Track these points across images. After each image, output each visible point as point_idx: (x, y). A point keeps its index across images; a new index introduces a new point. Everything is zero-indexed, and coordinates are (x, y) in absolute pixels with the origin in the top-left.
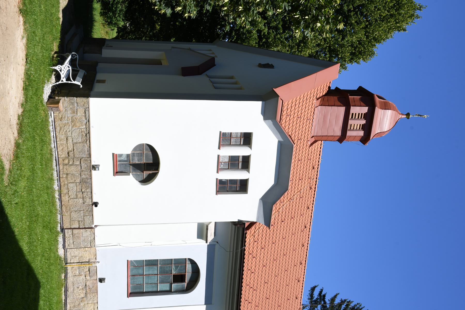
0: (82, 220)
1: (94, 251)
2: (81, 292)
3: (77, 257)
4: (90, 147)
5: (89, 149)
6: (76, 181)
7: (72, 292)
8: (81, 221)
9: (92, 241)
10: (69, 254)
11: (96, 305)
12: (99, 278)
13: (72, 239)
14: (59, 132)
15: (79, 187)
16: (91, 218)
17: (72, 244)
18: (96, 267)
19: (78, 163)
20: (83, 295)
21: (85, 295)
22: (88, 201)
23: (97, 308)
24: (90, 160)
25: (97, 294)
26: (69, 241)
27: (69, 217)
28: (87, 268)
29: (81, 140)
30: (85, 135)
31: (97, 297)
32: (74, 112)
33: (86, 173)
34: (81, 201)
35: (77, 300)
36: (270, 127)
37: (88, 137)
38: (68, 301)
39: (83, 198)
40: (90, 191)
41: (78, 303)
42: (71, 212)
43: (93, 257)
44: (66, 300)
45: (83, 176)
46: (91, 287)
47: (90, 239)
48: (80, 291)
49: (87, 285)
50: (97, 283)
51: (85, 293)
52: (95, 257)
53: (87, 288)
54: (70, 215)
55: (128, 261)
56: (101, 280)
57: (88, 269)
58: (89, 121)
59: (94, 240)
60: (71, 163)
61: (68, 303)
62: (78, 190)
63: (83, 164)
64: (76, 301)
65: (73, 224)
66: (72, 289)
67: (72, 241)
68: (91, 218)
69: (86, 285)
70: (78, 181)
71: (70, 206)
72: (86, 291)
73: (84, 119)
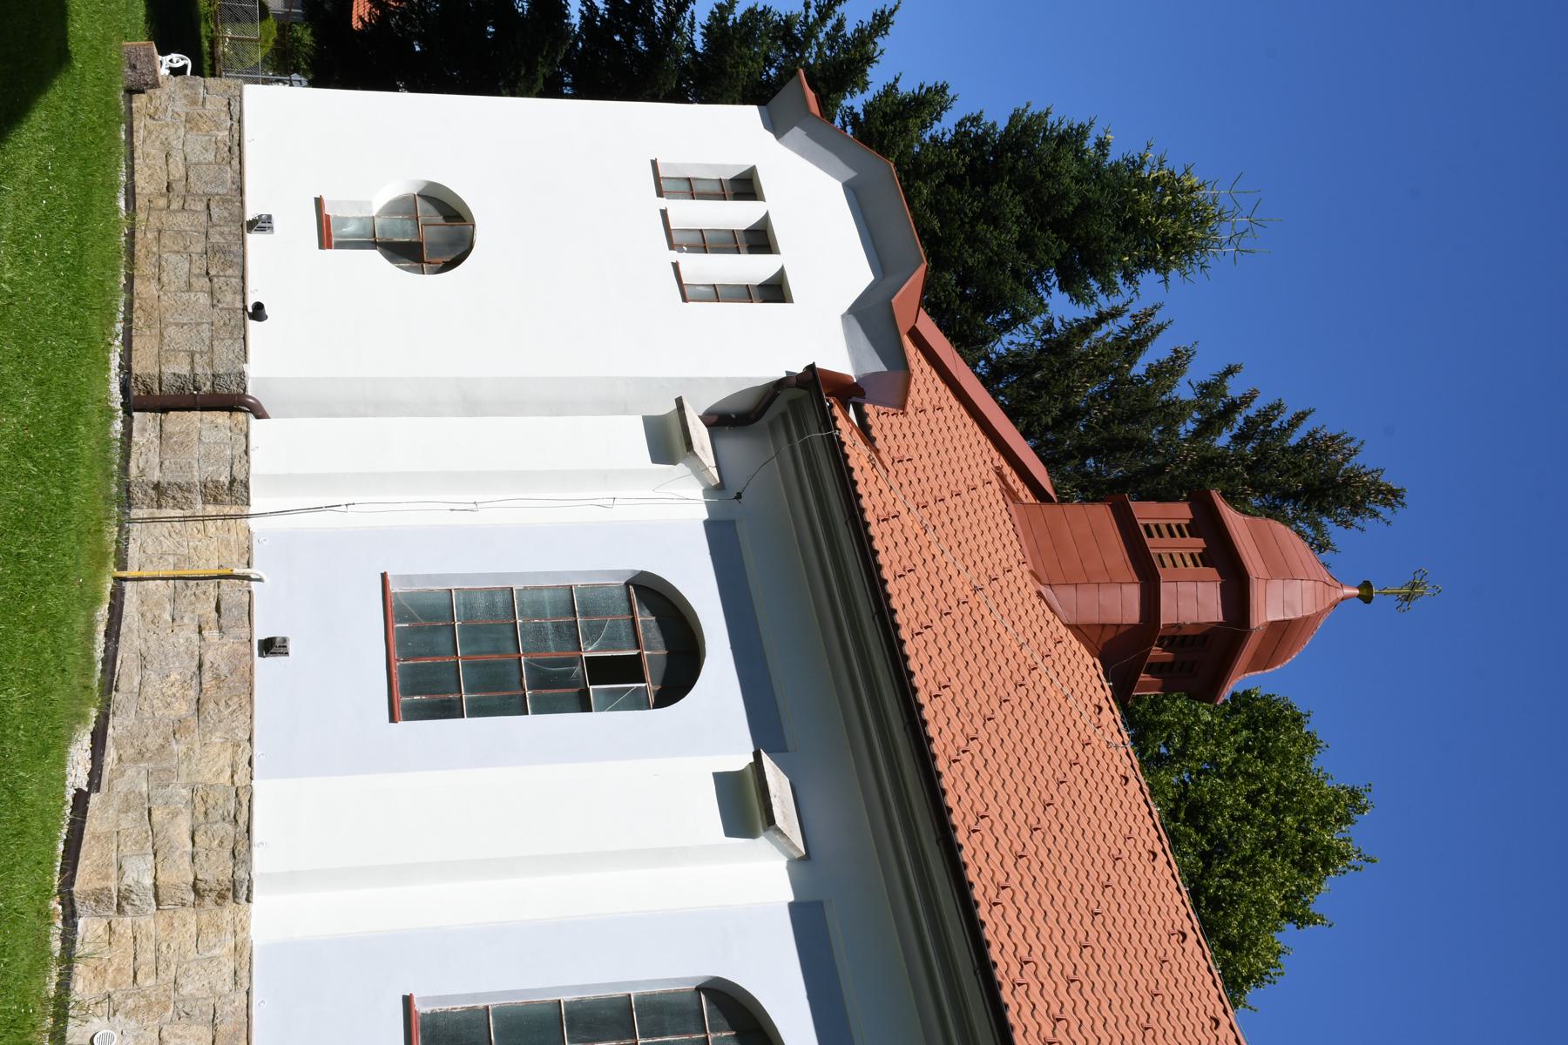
0: (205, 349)
1: (242, 538)
2: (178, 695)
3: (171, 559)
4: (241, 173)
5: (237, 177)
6: (192, 248)
7: (137, 690)
8: (201, 353)
9: (236, 461)
10: (138, 549)
11: (243, 751)
12: (260, 641)
13: (158, 450)
14: (144, 141)
15: (199, 265)
16: (238, 345)
17: (158, 469)
18: (248, 595)
19: (201, 206)
20: (185, 707)
21: (195, 707)
22: (230, 299)
23: (250, 763)
24: (242, 203)
25: (251, 702)
26: (143, 456)
27: (155, 341)
28: (212, 599)
29: (213, 158)
30: (226, 149)
31: (248, 714)
32: (194, 103)
33: (226, 229)
34: (204, 299)
35: (156, 728)
36: (802, 152)
37: (237, 153)
38: (110, 731)
39: (212, 293)
40: (238, 273)
41: (160, 741)
42: (167, 326)
43: (235, 557)
44: (110, 660)
45: (216, 238)
46: (224, 670)
47: (229, 452)
48: (174, 690)
49: (207, 665)
50: (252, 655)
51: (195, 700)
52: (247, 556)
53: (207, 676)
54: (161, 334)
55: (384, 576)
56: (270, 647)
57: (214, 605)
58: (240, 121)
59: (243, 455)
60: (174, 206)
61: (109, 742)
62: (197, 271)
63: (215, 211)
64: (152, 731)
65: (168, 361)
66: (137, 680)
67: (157, 460)
68: (237, 346)
69: (200, 666)
70: (199, 248)
71: (162, 311)
72: (201, 691)
73: (224, 116)
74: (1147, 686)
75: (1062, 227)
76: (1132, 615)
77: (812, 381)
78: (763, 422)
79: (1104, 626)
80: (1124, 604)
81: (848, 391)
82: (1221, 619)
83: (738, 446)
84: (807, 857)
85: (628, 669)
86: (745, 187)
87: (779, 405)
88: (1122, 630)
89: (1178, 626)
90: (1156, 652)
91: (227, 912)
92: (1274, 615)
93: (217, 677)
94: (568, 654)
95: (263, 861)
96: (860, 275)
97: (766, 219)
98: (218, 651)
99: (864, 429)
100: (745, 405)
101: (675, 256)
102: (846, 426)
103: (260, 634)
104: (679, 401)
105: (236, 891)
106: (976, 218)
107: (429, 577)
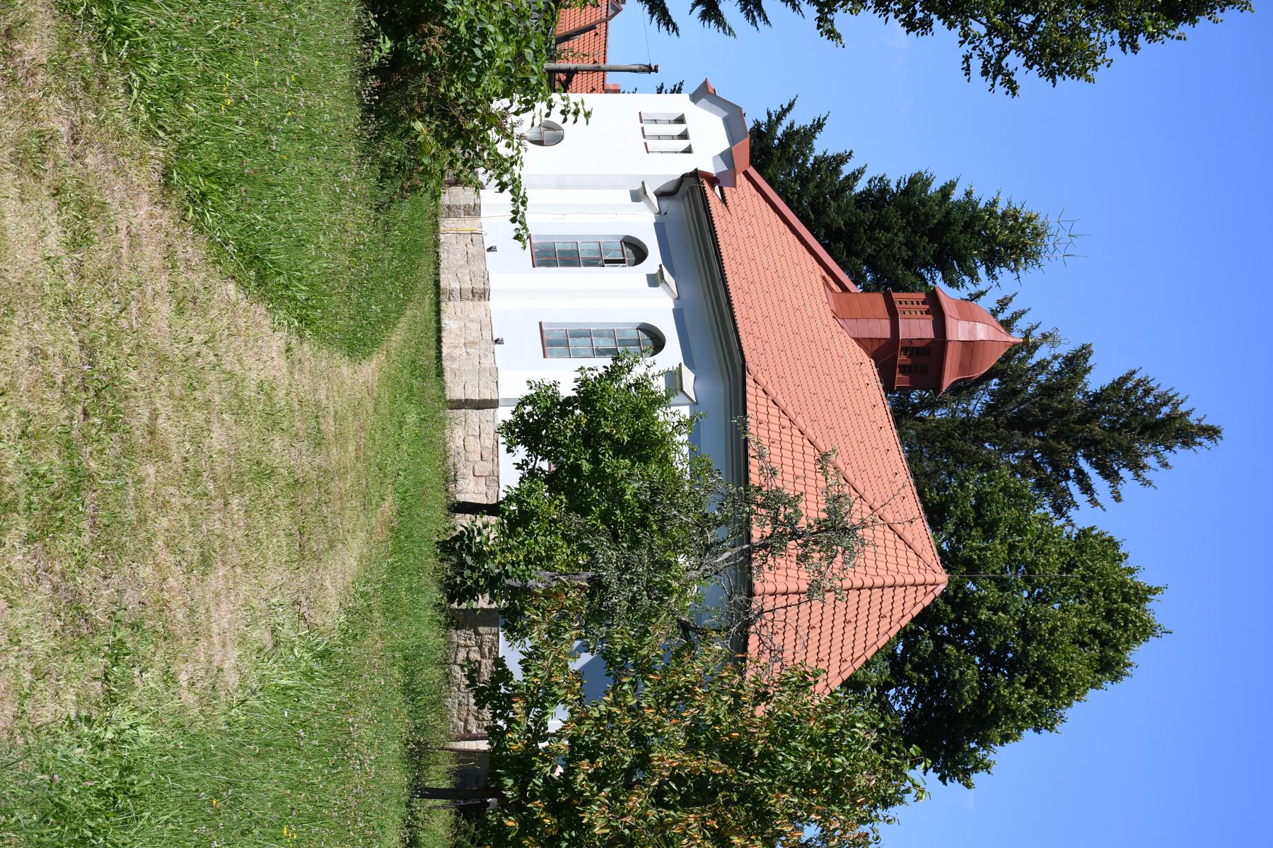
36: (705, 108)
53: (470, 255)
74: (900, 379)
75: (934, 235)
76: (887, 334)
77: (696, 174)
78: (678, 195)
79: (871, 339)
80: (882, 329)
81: (713, 181)
82: (932, 336)
83: (666, 203)
84: (678, 298)
85: (622, 261)
86: (680, 120)
87: (685, 188)
88: (883, 342)
89: (911, 340)
90: (902, 358)
91: (482, 303)
92: (963, 336)
93: (473, 256)
94: (599, 256)
95: (494, 285)
96: (724, 144)
97: (686, 131)
98: (472, 249)
99: (724, 200)
100: (671, 188)
101: (645, 140)
102: (713, 195)
103: (487, 246)
104: (643, 183)
105: (482, 294)
106: (872, 227)
107: (546, 236)
